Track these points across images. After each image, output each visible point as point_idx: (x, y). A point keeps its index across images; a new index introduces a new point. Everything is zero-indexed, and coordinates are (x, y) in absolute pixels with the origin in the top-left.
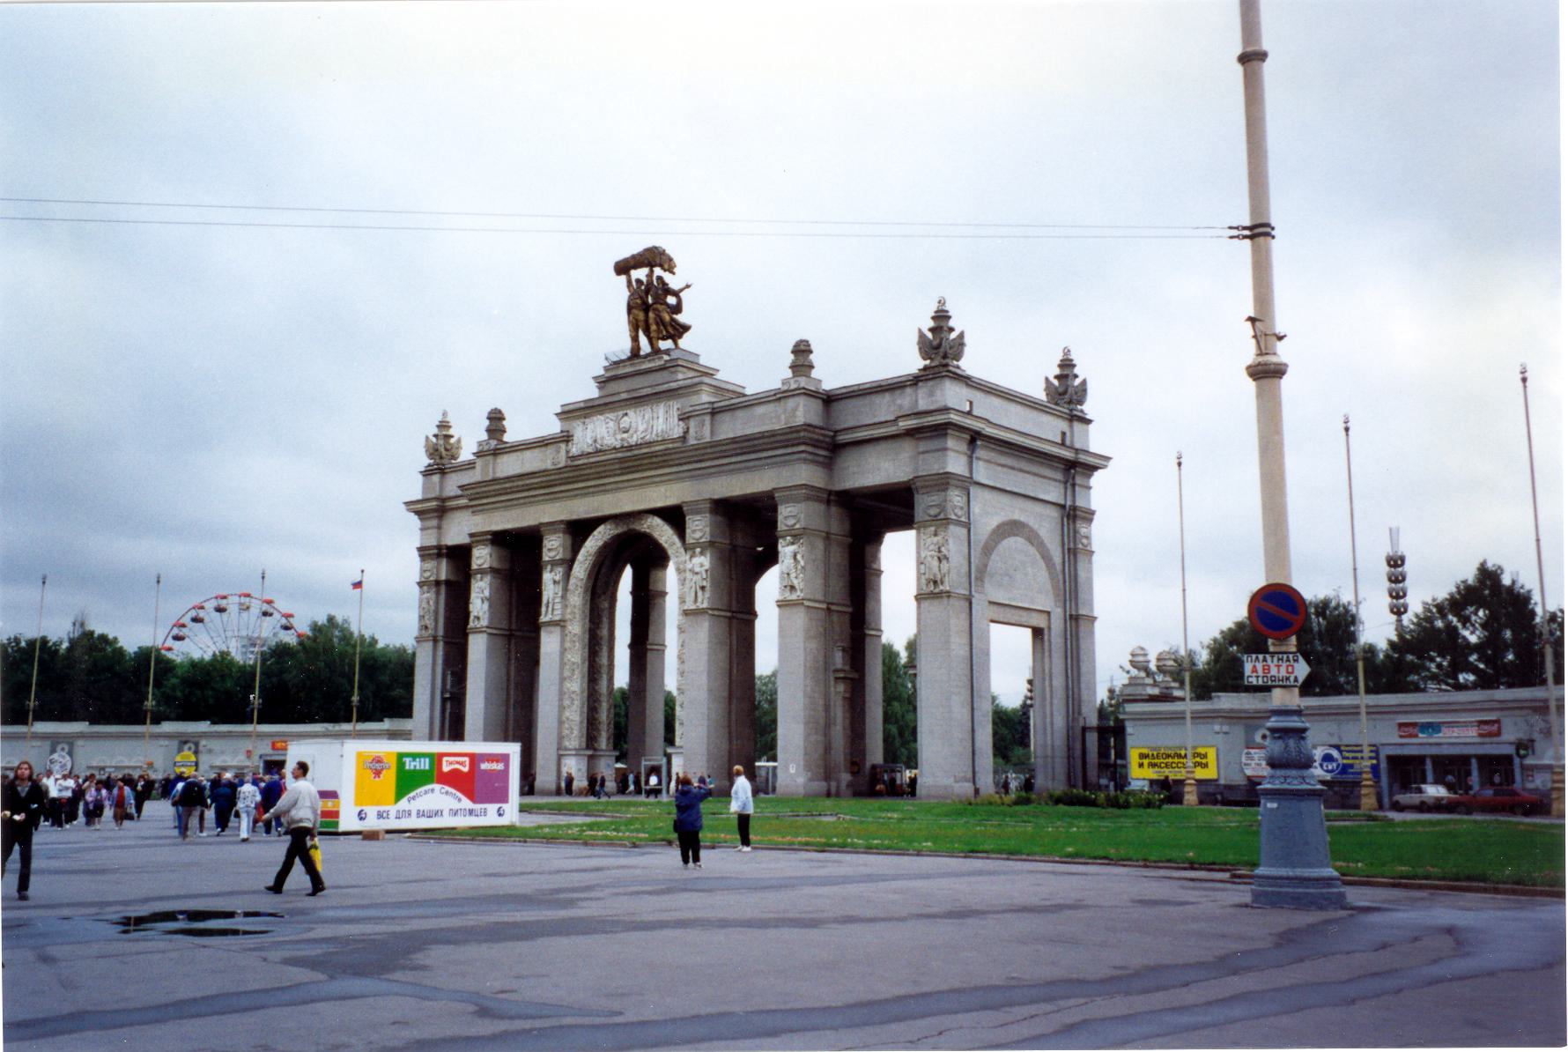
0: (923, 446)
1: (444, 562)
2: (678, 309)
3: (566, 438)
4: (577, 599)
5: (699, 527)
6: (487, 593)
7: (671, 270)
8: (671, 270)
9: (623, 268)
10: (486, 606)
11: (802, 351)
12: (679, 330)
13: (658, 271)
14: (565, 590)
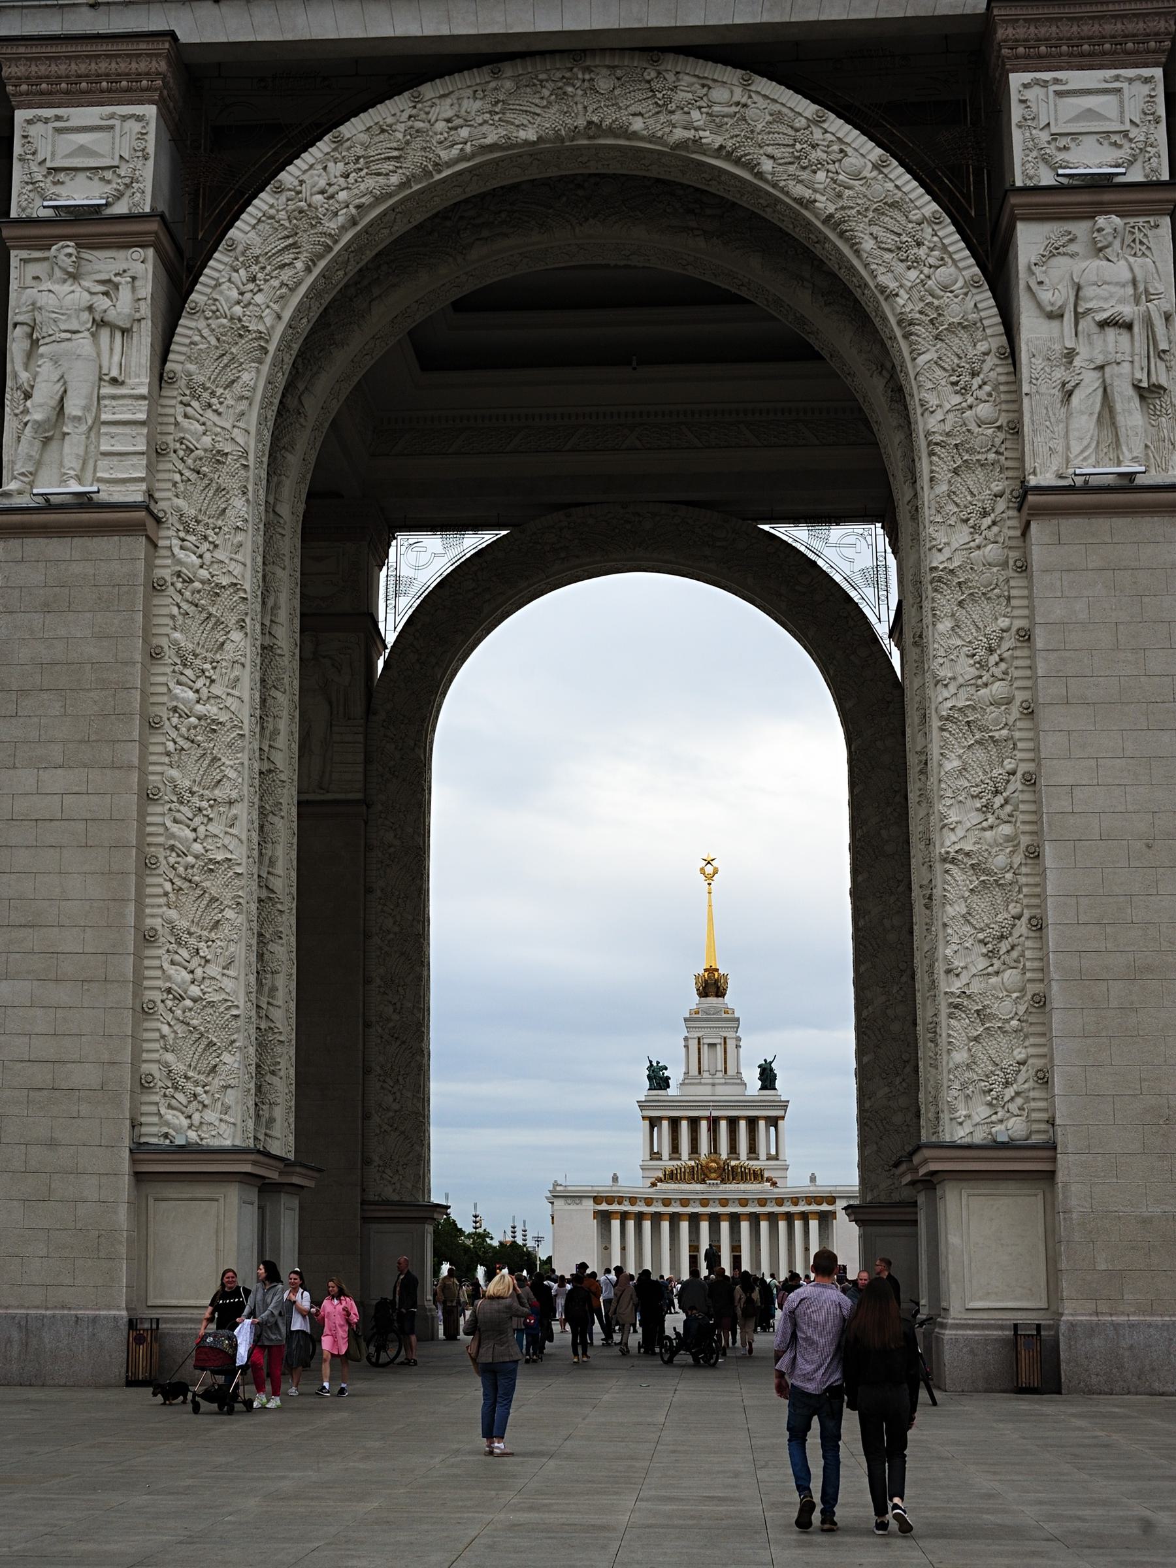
14: (161, 378)
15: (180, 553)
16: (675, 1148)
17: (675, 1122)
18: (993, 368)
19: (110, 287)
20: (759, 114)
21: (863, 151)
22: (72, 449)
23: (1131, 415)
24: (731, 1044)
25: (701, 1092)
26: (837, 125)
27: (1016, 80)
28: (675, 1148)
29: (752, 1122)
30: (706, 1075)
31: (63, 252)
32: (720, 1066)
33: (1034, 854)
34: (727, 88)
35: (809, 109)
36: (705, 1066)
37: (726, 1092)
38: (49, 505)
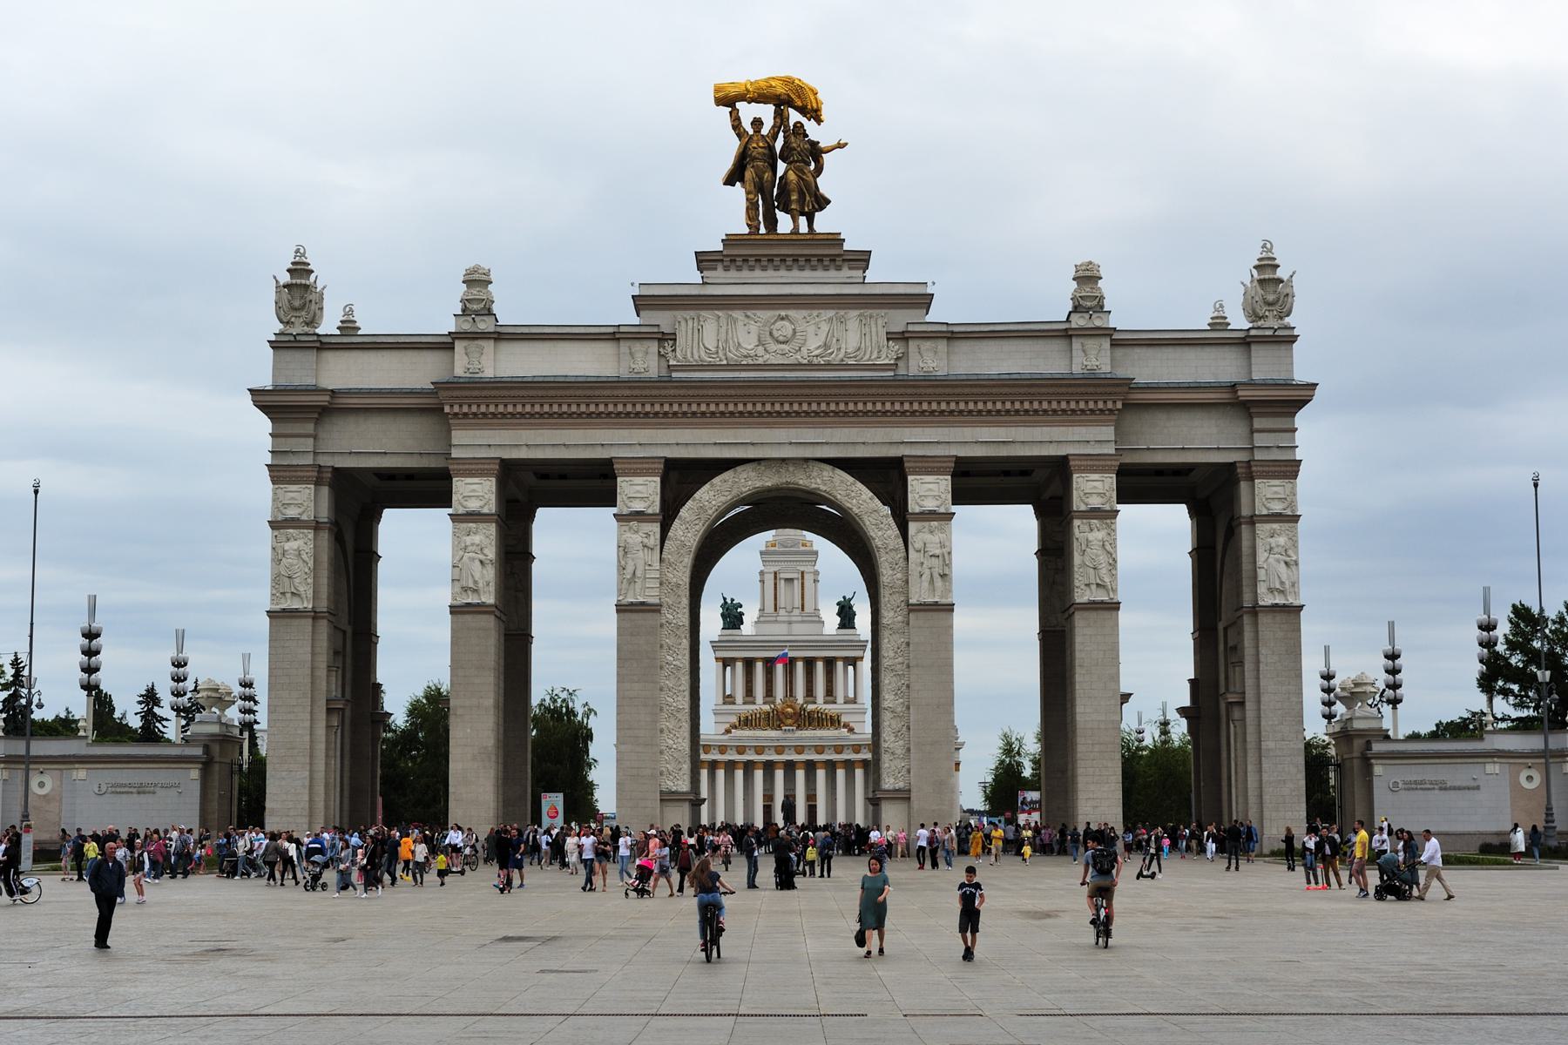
0: (1258, 423)
1: (325, 490)
2: (819, 170)
3: (665, 338)
4: (683, 576)
5: (927, 491)
6: (491, 553)
7: (819, 121)
8: (819, 121)
9: (727, 100)
10: (490, 574)
11: (1087, 277)
12: (822, 202)
13: (794, 116)
15: (667, 615)
16: (749, 691)
17: (749, 664)
18: (902, 563)
19: (648, 536)
20: (837, 480)
21: (866, 493)
22: (638, 586)
23: (939, 582)
24: (809, 579)
25: (777, 631)
26: (859, 485)
27: (910, 478)
28: (749, 691)
29: (830, 663)
30: (782, 612)
31: (634, 524)
32: (798, 603)
33: (908, 708)
34: (828, 471)
35: (851, 479)
36: (782, 602)
37: (802, 631)
38: (632, 604)
